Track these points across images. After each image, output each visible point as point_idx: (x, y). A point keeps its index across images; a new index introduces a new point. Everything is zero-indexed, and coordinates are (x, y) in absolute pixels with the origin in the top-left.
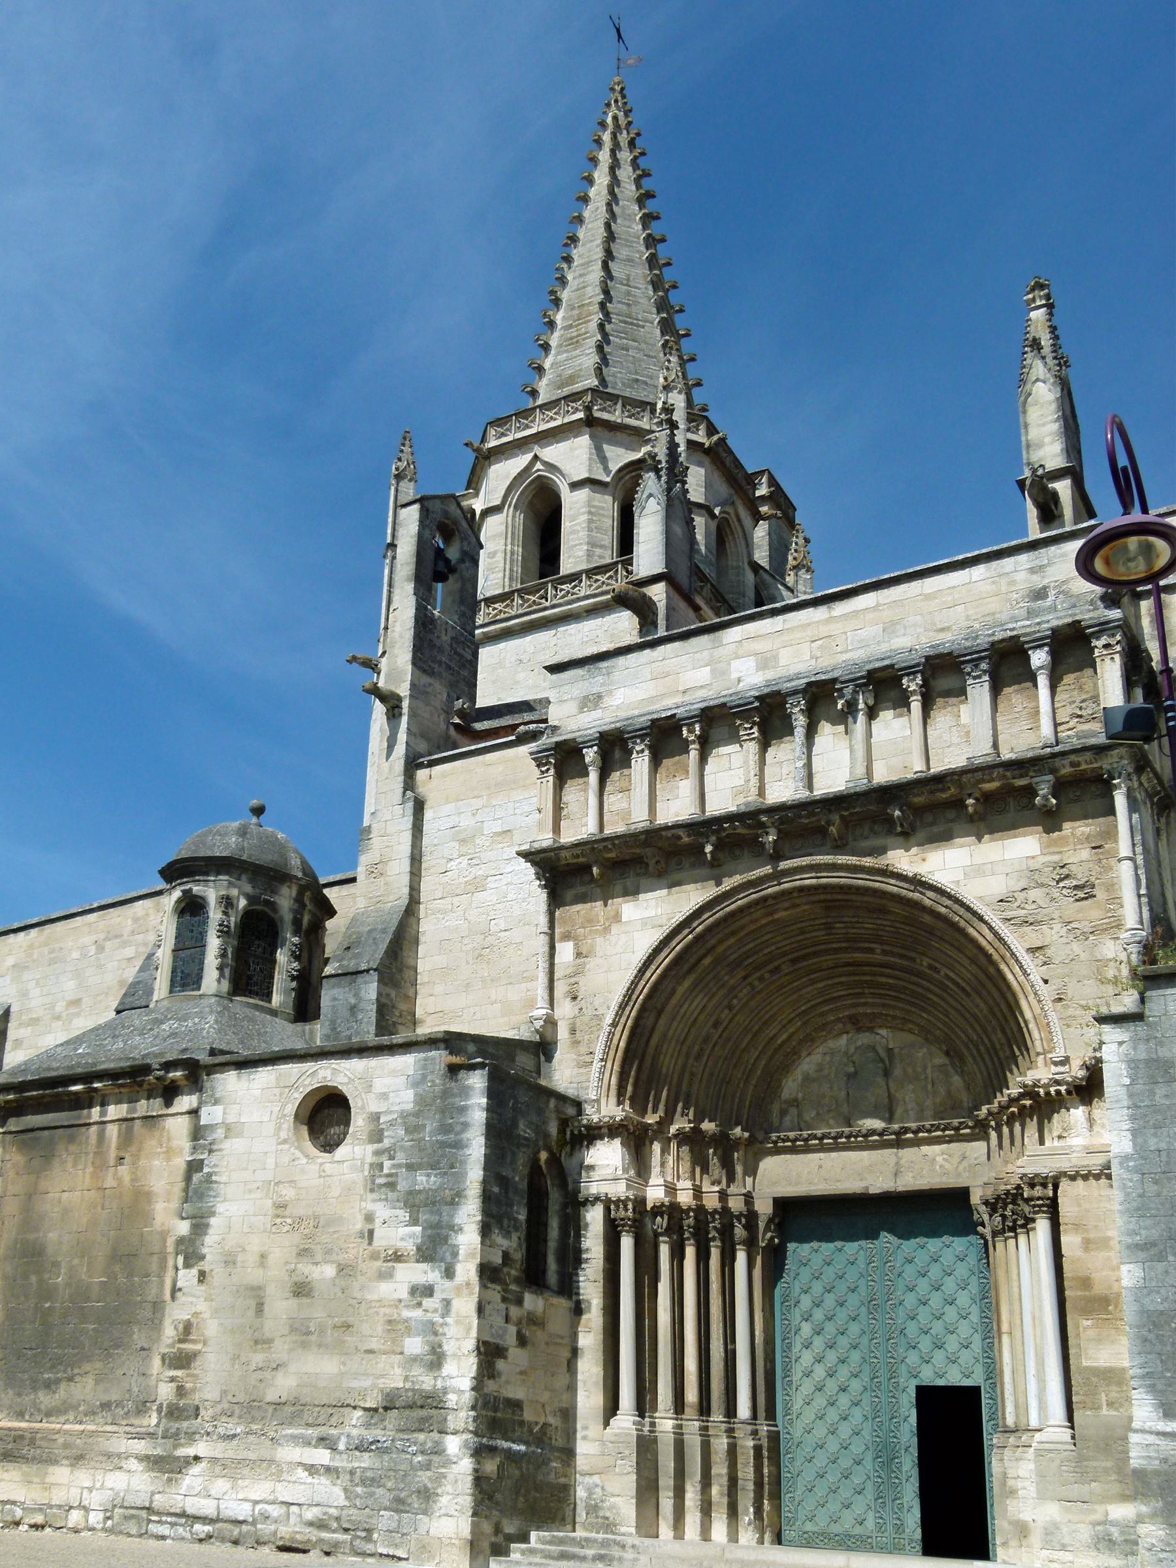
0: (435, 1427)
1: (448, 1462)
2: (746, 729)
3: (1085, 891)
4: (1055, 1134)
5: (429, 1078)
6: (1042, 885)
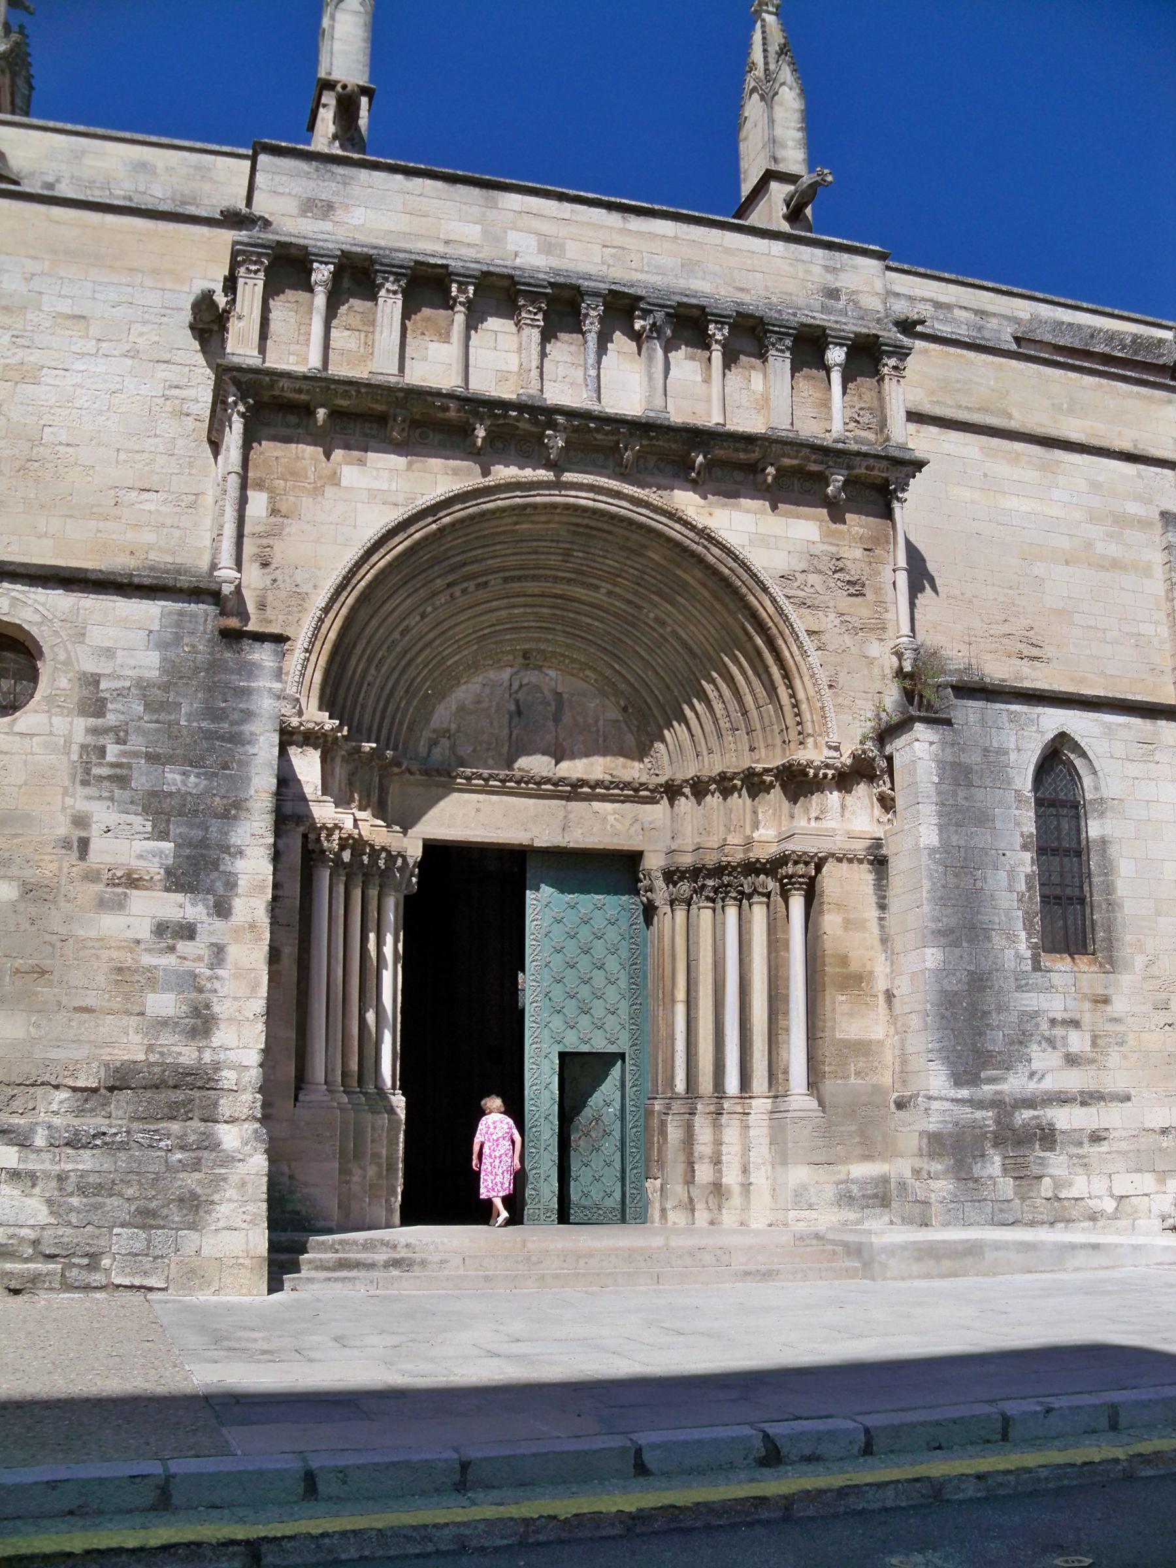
0: (197, 1113)
1: (228, 1160)
3: (856, 588)
4: (813, 815)
5: (186, 640)
6: (820, 572)
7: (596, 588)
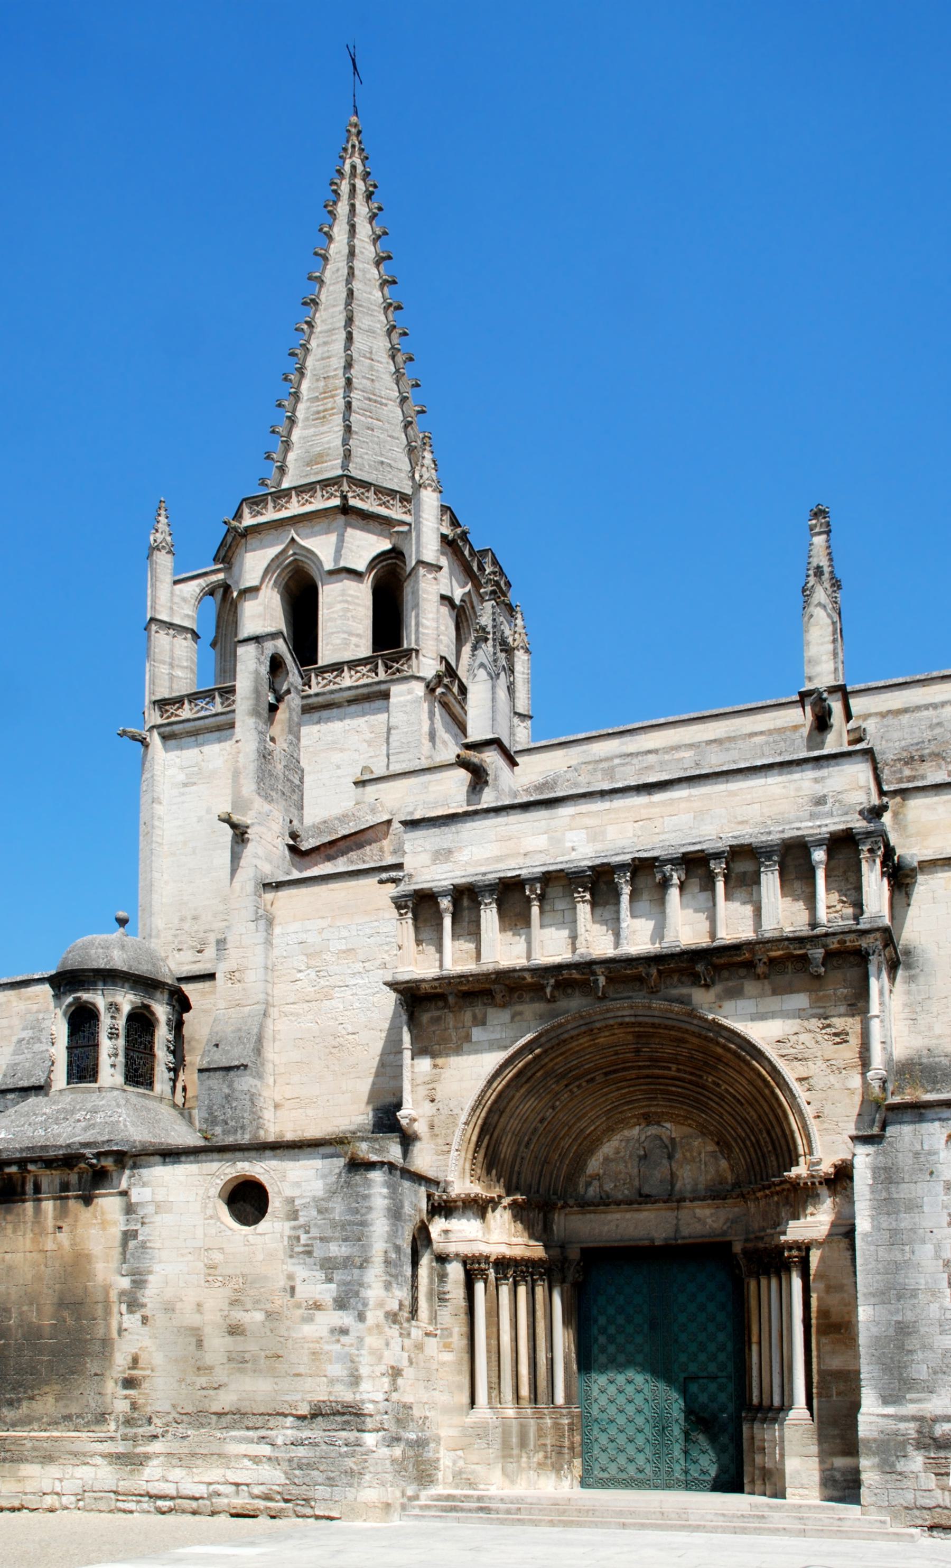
2: (579, 892)
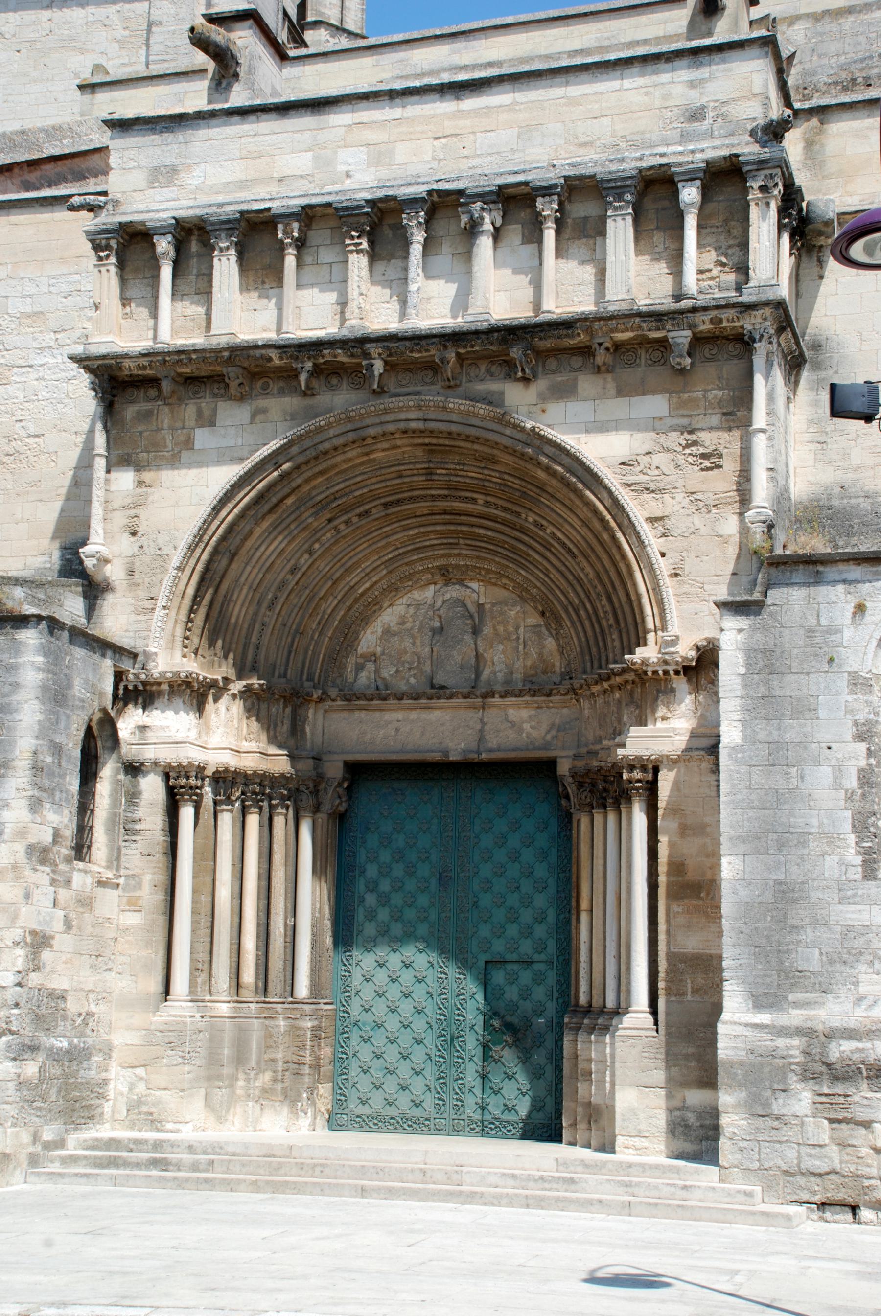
2: (352, 238)
6: (668, 450)
7: (474, 501)
